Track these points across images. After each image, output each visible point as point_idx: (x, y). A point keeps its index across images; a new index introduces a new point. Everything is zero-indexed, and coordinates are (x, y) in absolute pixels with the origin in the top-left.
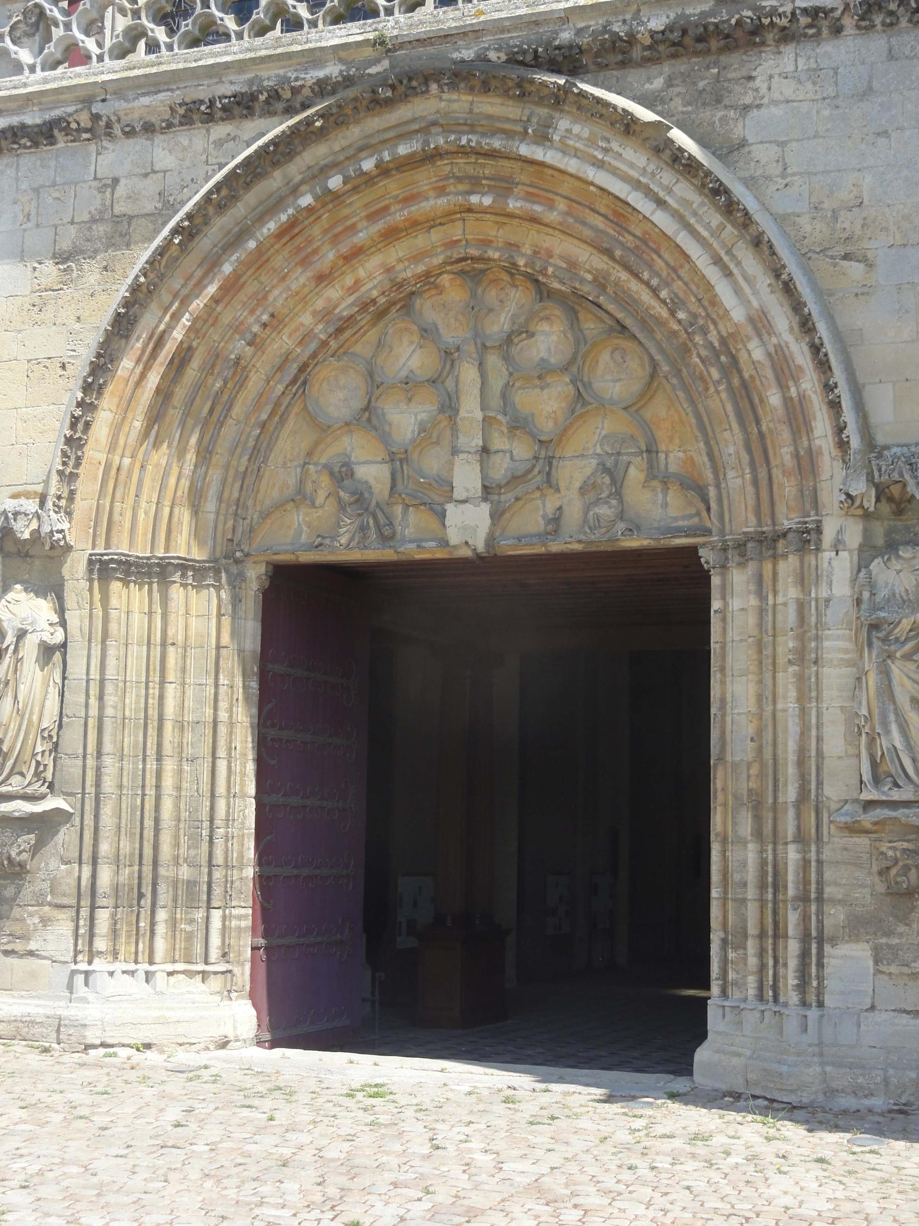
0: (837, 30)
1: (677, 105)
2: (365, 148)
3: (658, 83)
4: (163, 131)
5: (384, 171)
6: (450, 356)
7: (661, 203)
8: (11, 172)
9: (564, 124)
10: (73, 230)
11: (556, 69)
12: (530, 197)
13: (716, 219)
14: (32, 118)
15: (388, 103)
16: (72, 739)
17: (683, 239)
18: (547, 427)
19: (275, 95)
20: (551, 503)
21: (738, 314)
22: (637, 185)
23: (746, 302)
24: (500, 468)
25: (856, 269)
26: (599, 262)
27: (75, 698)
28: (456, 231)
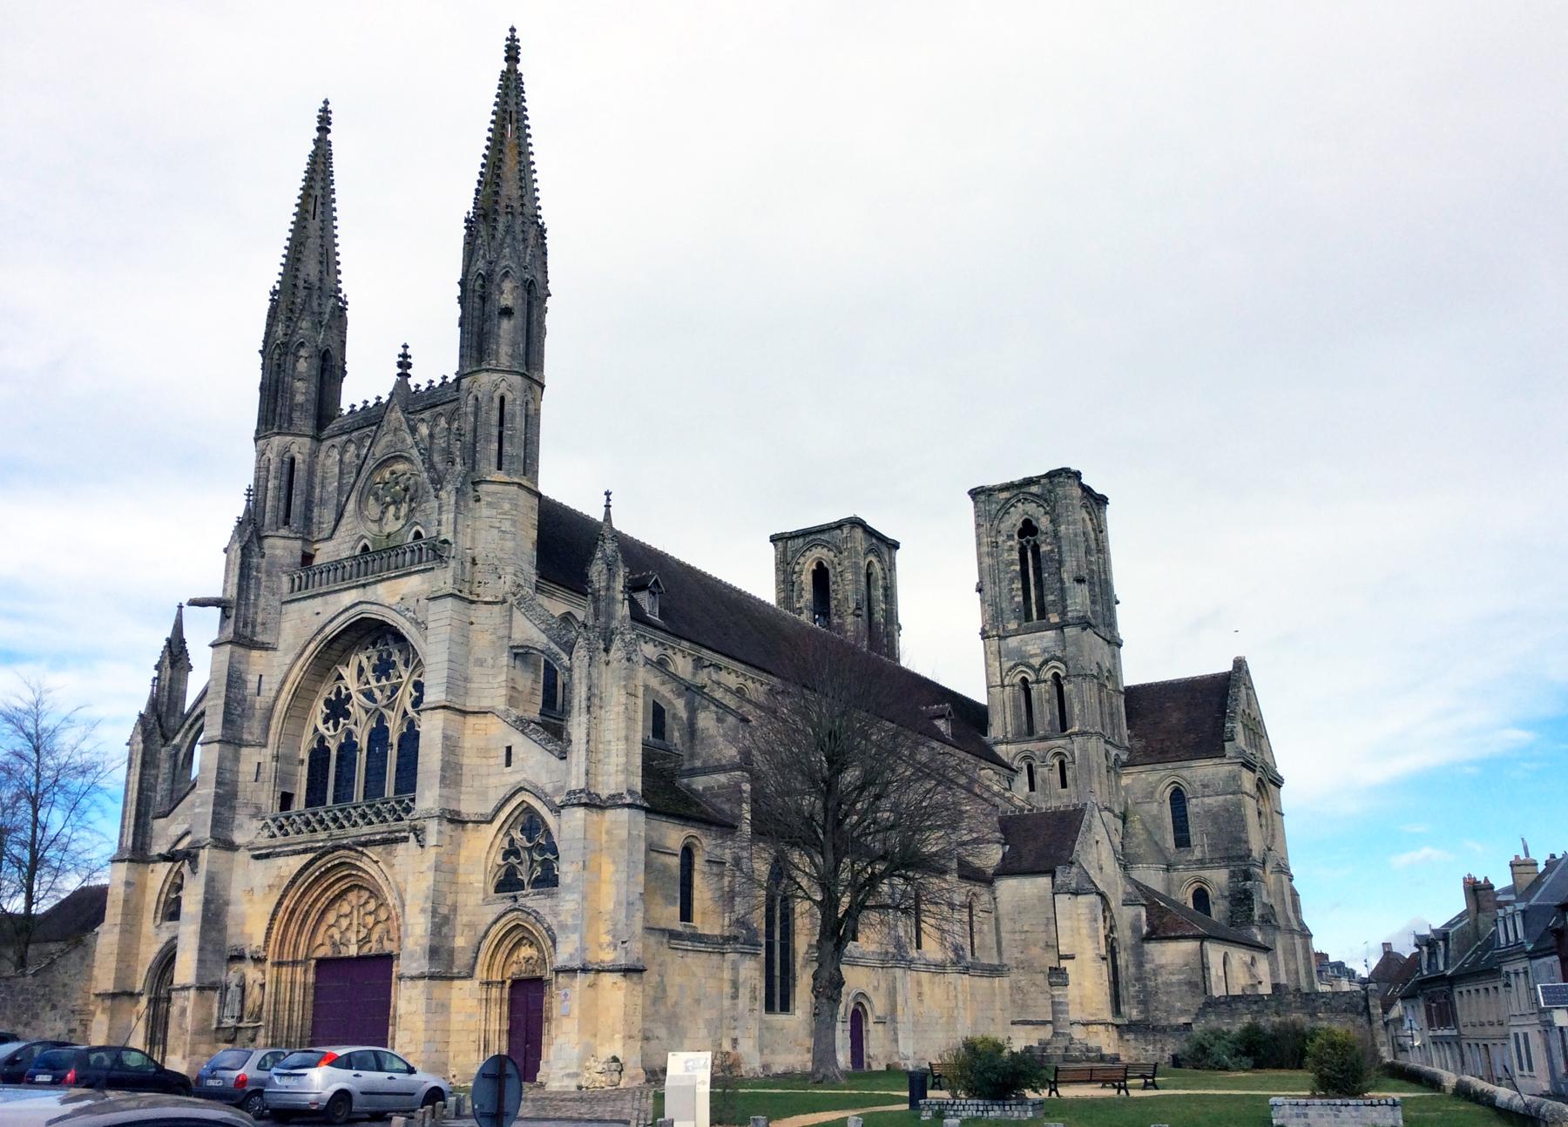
11: (359, 845)
14: (264, 851)
15: (333, 852)
16: (265, 1007)
20: (368, 946)
24: (362, 935)
27: (266, 997)
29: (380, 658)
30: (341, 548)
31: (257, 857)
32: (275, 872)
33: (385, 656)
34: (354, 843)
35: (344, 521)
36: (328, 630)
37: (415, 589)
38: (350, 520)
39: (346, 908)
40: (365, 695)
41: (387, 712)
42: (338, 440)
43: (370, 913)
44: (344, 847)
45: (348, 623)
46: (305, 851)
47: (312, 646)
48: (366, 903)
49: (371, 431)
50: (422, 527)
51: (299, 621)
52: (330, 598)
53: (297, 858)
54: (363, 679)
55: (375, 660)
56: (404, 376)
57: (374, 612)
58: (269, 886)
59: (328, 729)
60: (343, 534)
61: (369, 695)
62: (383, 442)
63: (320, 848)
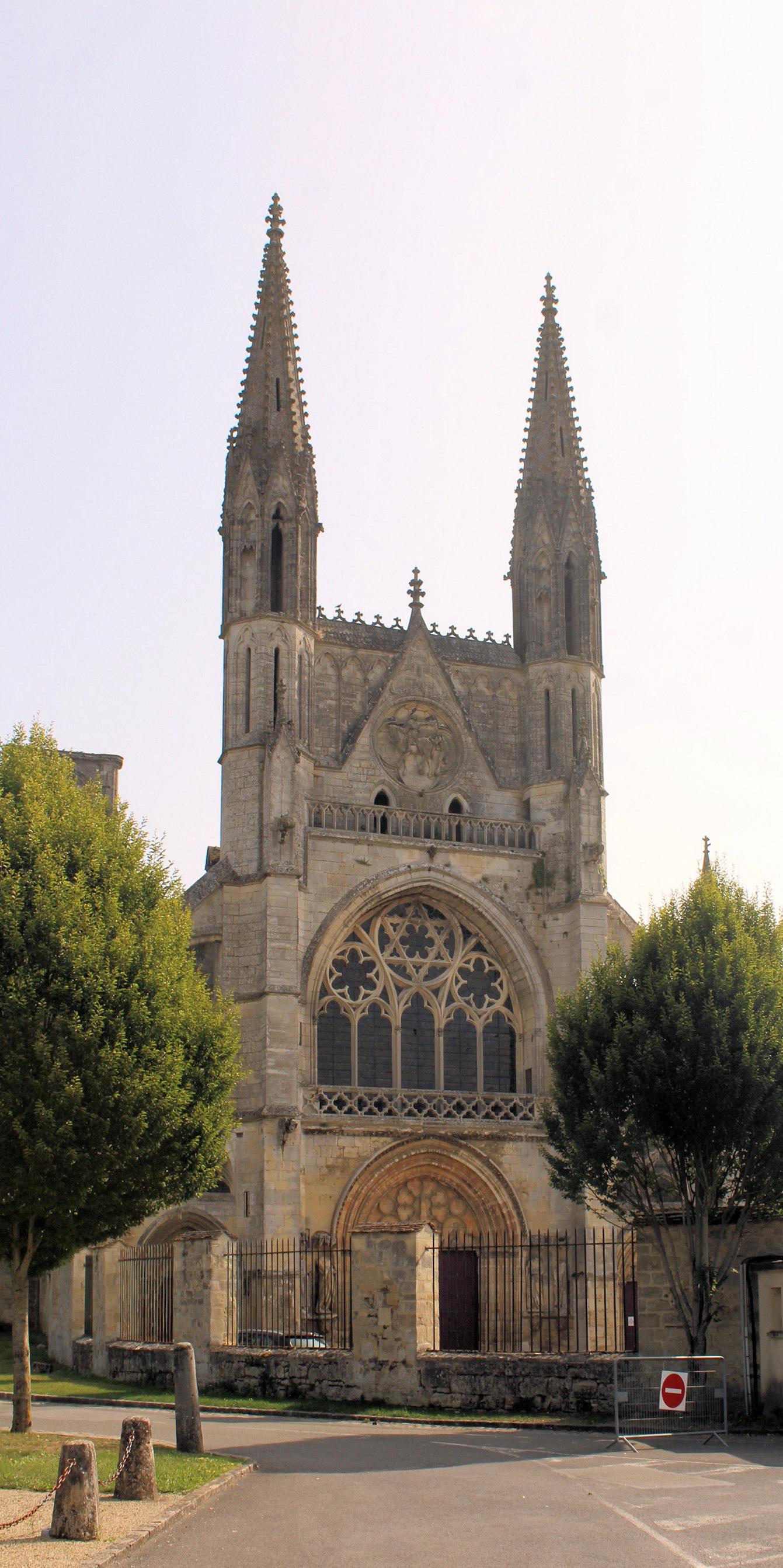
0: (522, 1140)
1: (488, 1151)
2: (413, 1149)
3: (483, 1145)
4: (358, 1136)
5: (416, 1154)
6: (419, 1199)
7: (483, 1173)
8: (311, 1140)
9: (462, 1151)
10: (332, 1160)
12: (446, 1164)
13: (496, 1180)
17: (488, 1183)
18: (440, 1219)
19: (391, 1133)
21: (500, 1202)
22: (478, 1169)
23: (502, 1199)
25: (525, 1195)
26: (458, 1182)
28: (424, 1169)
29: (410, 929)
30: (355, 786)
31: (308, 1132)
32: (338, 1153)
33: (417, 928)
34: (453, 1135)
35: (355, 754)
36: (382, 887)
37: (500, 873)
38: (364, 756)
39: (404, 1198)
40: (391, 966)
41: (428, 997)
42: (336, 650)
43: (439, 1206)
44: (442, 1138)
45: (410, 886)
46: (383, 1134)
47: (359, 901)
48: (434, 1194)
49: (386, 658)
50: (466, 797)
51: (335, 865)
52: (382, 851)
53: (368, 1140)
54: (389, 950)
55: (402, 932)
56: (416, 606)
57: (446, 882)
58: (328, 1167)
59: (343, 995)
60: (355, 770)
61: (400, 969)
62: (404, 675)
63: (405, 1133)
